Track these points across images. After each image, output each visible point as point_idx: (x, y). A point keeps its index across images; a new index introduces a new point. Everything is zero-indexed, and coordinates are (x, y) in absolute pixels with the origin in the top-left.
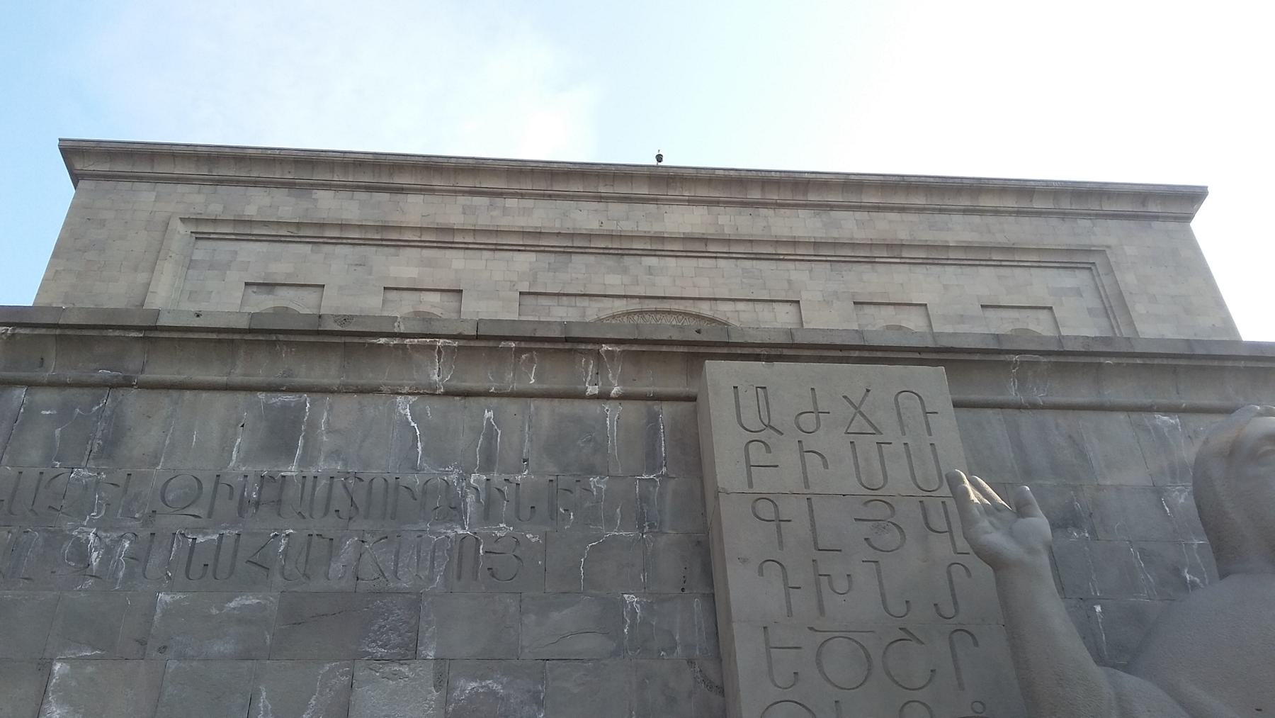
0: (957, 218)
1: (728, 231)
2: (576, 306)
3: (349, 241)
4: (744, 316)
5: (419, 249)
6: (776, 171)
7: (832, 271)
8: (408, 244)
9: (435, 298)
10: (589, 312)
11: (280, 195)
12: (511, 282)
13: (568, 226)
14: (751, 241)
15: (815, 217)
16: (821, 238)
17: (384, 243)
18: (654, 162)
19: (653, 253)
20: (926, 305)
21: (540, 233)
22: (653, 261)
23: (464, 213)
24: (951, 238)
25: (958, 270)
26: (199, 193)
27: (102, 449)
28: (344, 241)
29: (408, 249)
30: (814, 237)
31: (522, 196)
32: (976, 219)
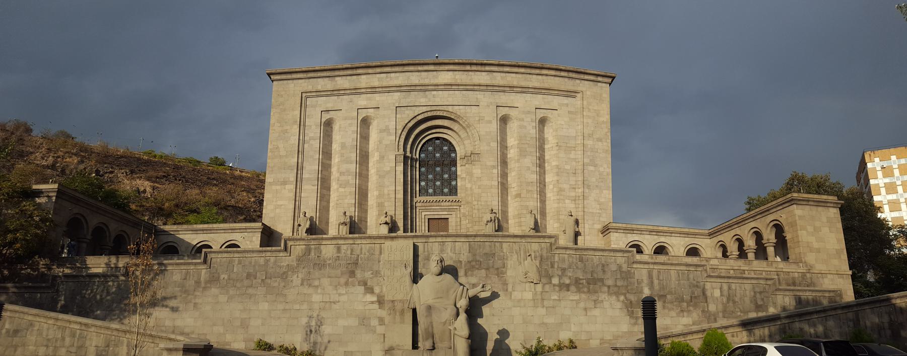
1: (459, 82)
4: (462, 111)
13: (409, 83)
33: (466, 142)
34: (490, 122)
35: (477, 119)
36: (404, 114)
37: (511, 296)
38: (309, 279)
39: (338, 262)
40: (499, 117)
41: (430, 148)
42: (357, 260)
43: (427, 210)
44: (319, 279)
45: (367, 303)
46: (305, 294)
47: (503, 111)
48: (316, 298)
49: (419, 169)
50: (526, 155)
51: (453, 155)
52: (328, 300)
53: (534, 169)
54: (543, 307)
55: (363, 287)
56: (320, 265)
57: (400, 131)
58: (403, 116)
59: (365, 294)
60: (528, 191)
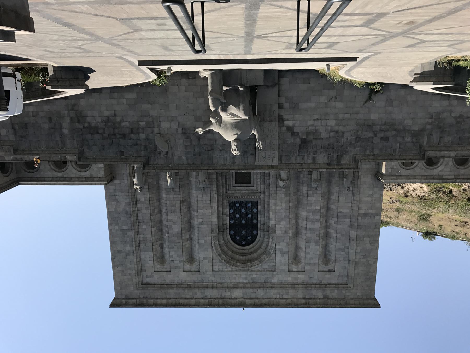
4: (225, 267)
5: (299, 282)
6: (216, 307)
8: (301, 284)
9: (294, 269)
10: (260, 267)
11: (330, 296)
18: (244, 308)
22: (246, 281)
23: (289, 293)
25: (174, 282)
26: (348, 296)
29: (301, 282)
30: (208, 289)
31: (276, 298)
32: (168, 296)
33: (222, 242)
34: (205, 259)
35: (214, 261)
37: (179, 125)
41: (249, 238)
42: (299, 152)
43: (252, 190)
44: (330, 137)
46: (341, 126)
47: (194, 267)
48: (332, 123)
51: (232, 232)
52: (323, 121)
53: (170, 224)
54: (152, 116)
55: (295, 131)
56: (329, 148)
58: (269, 264)
59: (293, 126)
60: (174, 205)
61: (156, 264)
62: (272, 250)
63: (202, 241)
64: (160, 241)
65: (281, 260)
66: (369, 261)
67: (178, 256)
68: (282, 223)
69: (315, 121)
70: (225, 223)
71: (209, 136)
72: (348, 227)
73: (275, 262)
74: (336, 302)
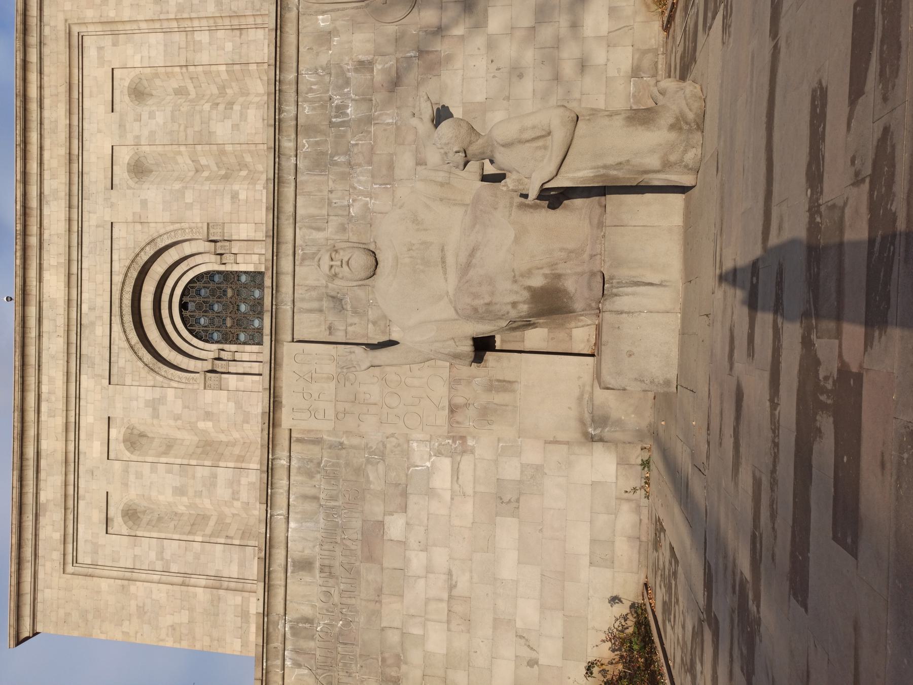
0: (46, 114)
1: (63, 259)
2: (118, 353)
3: (76, 480)
4: (123, 256)
7: (89, 199)
9: (113, 432)
11: (43, 521)
12: (102, 389)
13: (62, 357)
14: (69, 247)
15: (49, 205)
16: (66, 204)
17: (77, 461)
19: (79, 306)
20: (112, 146)
21: (67, 372)
23: (54, 416)
24: (63, 122)
26: (44, 565)
27: (309, 623)
28: (76, 483)
32: (47, 102)
34: (144, 203)
35: (138, 227)
36: (124, 368)
38: (384, 660)
39: (338, 570)
40: (131, 183)
45: (456, 487)
49: (240, 344)
50: (209, 132)
52: (444, 605)
53: (236, 116)
57: (159, 378)
59: (430, 493)
61: (133, 73)
62: (165, 377)
63: (189, 197)
64: (194, 87)
65: (137, 401)
66: (129, 620)
67: (152, 133)
68: (231, 405)
69: (444, 577)
70: (240, 258)
71: (406, 161)
72: (218, 570)
73: (134, 383)
74: (28, 535)
